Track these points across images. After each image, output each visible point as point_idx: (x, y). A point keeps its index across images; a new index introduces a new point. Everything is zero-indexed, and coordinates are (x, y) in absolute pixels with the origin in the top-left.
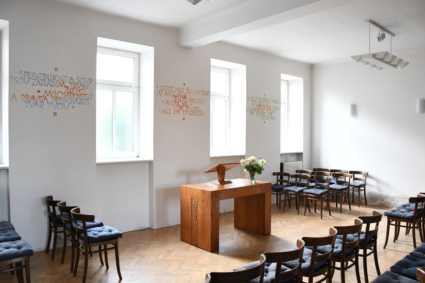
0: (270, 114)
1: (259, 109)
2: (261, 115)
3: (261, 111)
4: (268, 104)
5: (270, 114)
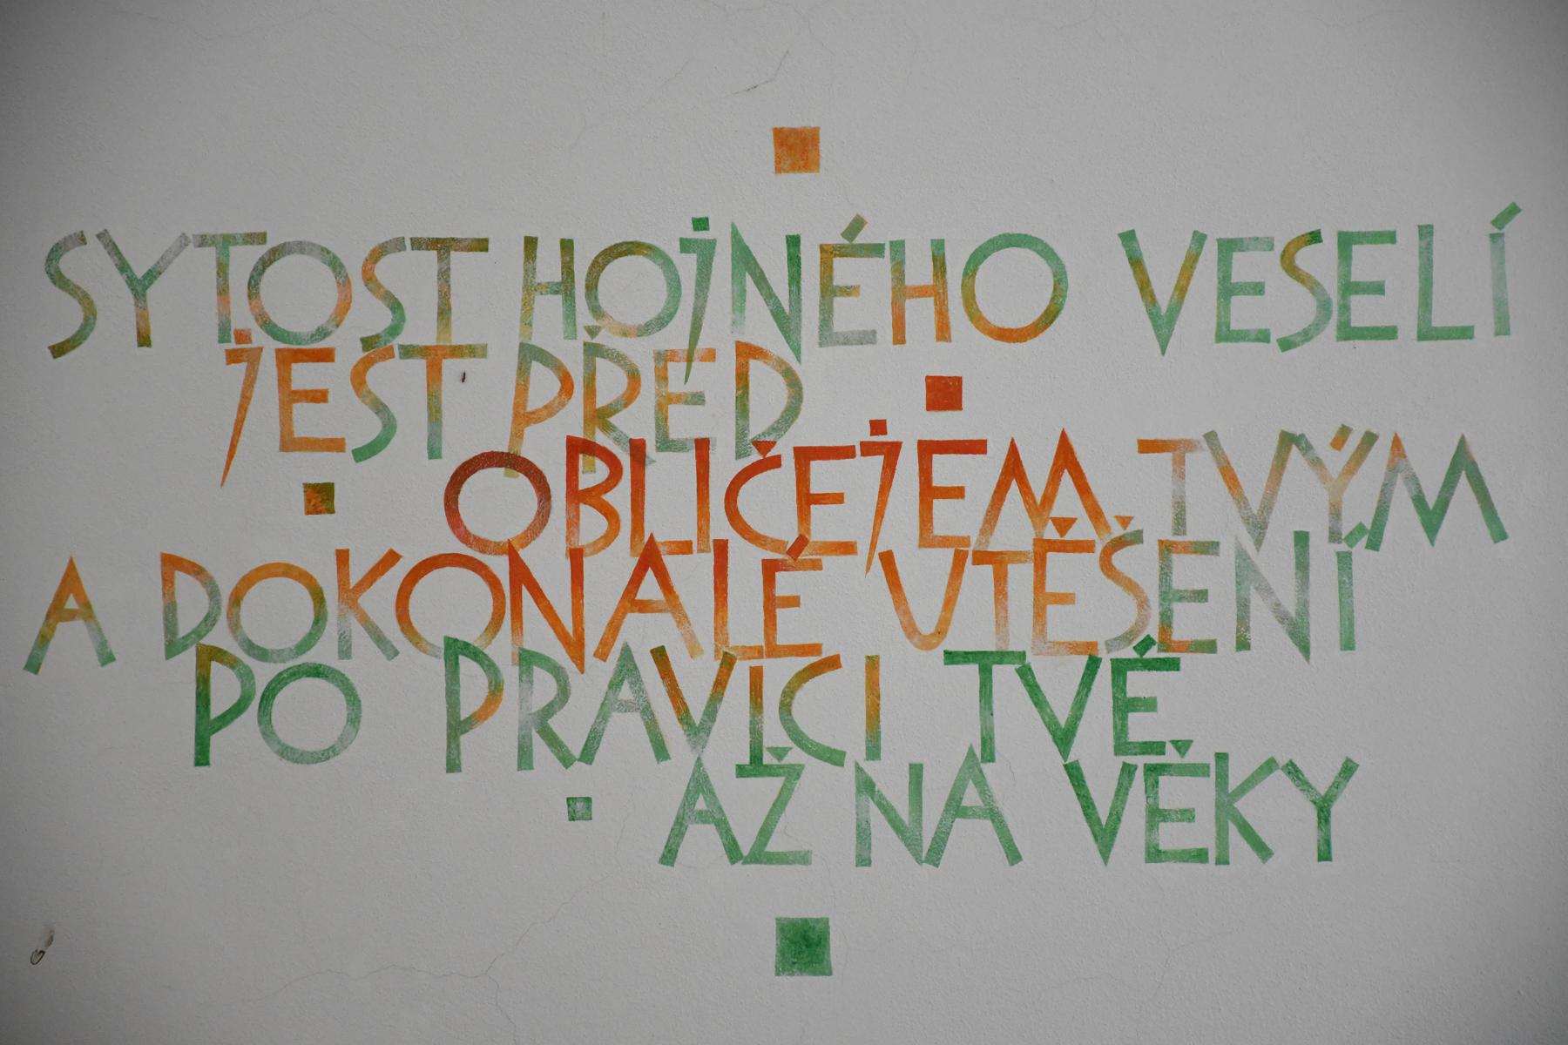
2: (626, 729)
3: (642, 633)
4: (944, 394)
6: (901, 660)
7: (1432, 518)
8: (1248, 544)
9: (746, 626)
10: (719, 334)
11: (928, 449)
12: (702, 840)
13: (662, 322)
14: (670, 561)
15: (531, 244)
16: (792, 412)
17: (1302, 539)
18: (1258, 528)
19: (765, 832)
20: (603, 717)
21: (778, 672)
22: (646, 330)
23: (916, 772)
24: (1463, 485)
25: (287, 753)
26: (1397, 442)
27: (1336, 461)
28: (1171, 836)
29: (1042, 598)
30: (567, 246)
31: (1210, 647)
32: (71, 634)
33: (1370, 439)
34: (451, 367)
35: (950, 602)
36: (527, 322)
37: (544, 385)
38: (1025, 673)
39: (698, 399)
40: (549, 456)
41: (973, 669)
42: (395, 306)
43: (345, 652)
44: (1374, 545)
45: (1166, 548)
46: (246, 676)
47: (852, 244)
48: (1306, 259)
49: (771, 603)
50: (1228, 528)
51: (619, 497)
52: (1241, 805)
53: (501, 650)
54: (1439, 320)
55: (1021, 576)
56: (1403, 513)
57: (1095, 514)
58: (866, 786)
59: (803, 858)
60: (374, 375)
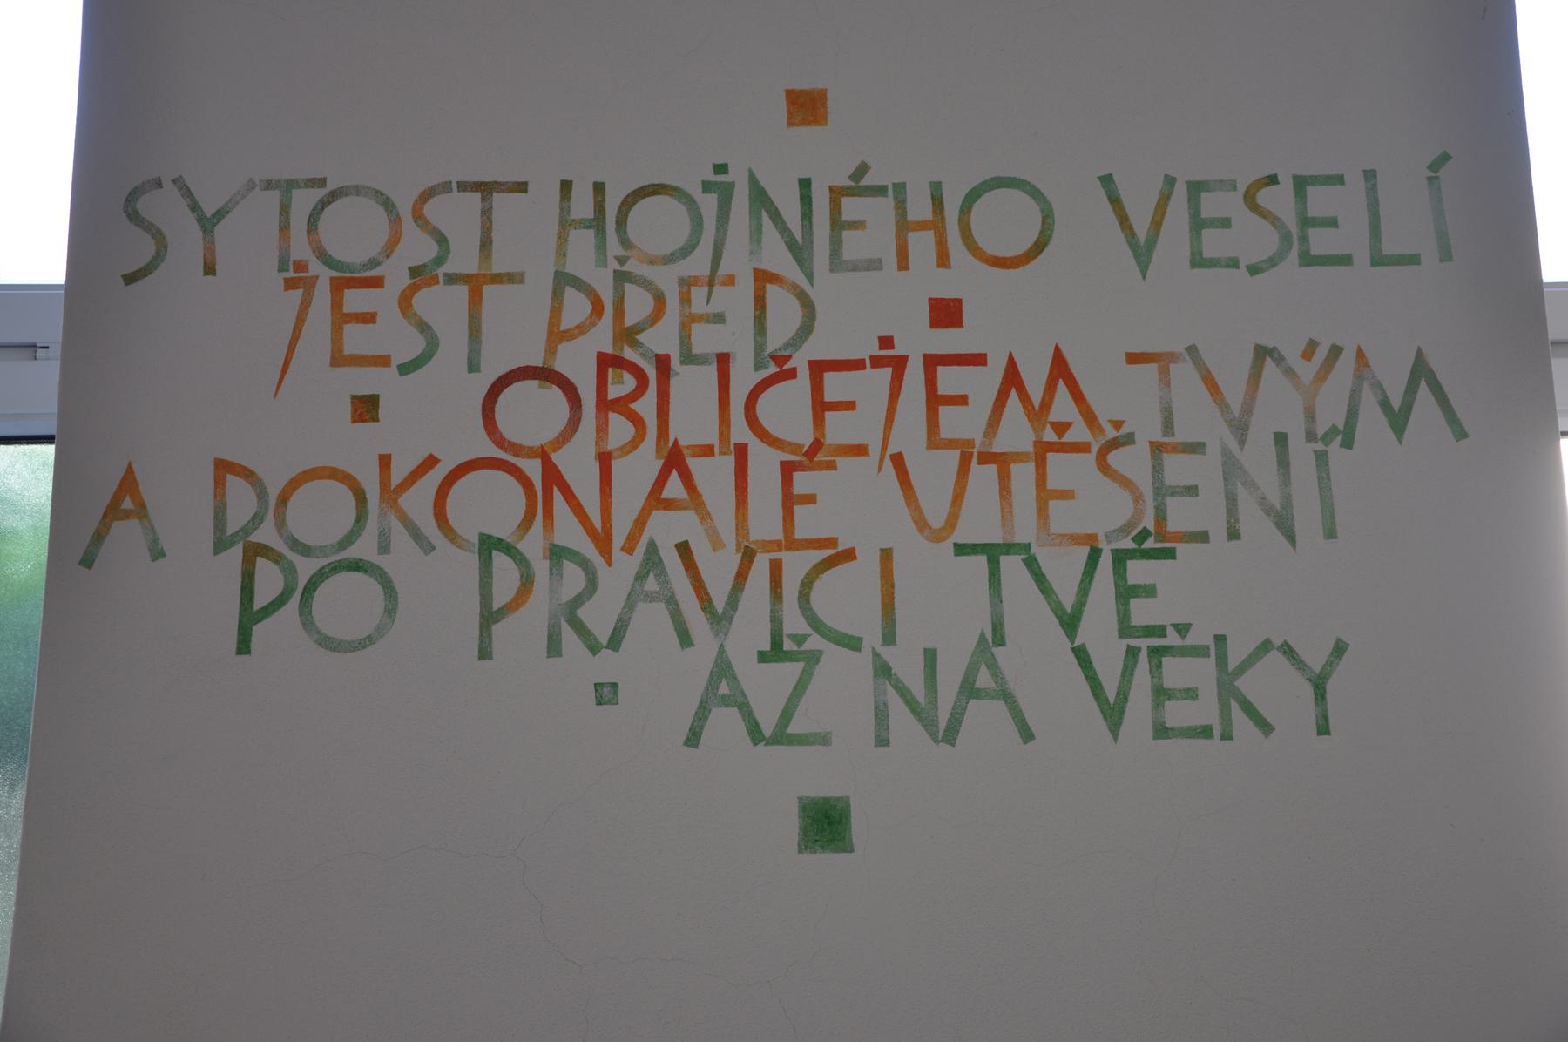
0: (1064, 568)
1: (577, 463)
3: (667, 528)
4: (946, 313)
5: (1064, 568)
6: (915, 555)
7: (1398, 421)
8: (1232, 444)
9: (766, 521)
10: (738, 261)
11: (932, 363)
12: (725, 722)
13: (685, 252)
14: (694, 464)
15: (566, 187)
16: (806, 330)
17: (1281, 439)
18: (1241, 429)
19: (786, 716)
20: (630, 605)
21: (796, 565)
22: (670, 259)
23: (931, 656)
24: (1424, 390)
25: (329, 643)
26: (1360, 354)
27: (1307, 371)
28: (1178, 714)
29: (1044, 495)
30: (599, 188)
31: (1203, 537)
32: (126, 533)
33: (1336, 352)
34: (488, 290)
35: (958, 498)
36: (561, 253)
37: (576, 307)
38: (1032, 564)
39: (719, 318)
40: (577, 363)
41: (981, 560)
42: (441, 240)
43: (384, 548)
44: (1348, 443)
45: (1157, 449)
46: (290, 571)
47: (858, 185)
48: (1265, 197)
49: (789, 500)
50: (1216, 433)
51: (646, 406)
52: (1244, 684)
53: (533, 545)
54: (1389, 248)
55: (1023, 475)
56: (1371, 420)
57: (1090, 418)
58: (883, 670)
59: (823, 739)
60: (421, 300)
